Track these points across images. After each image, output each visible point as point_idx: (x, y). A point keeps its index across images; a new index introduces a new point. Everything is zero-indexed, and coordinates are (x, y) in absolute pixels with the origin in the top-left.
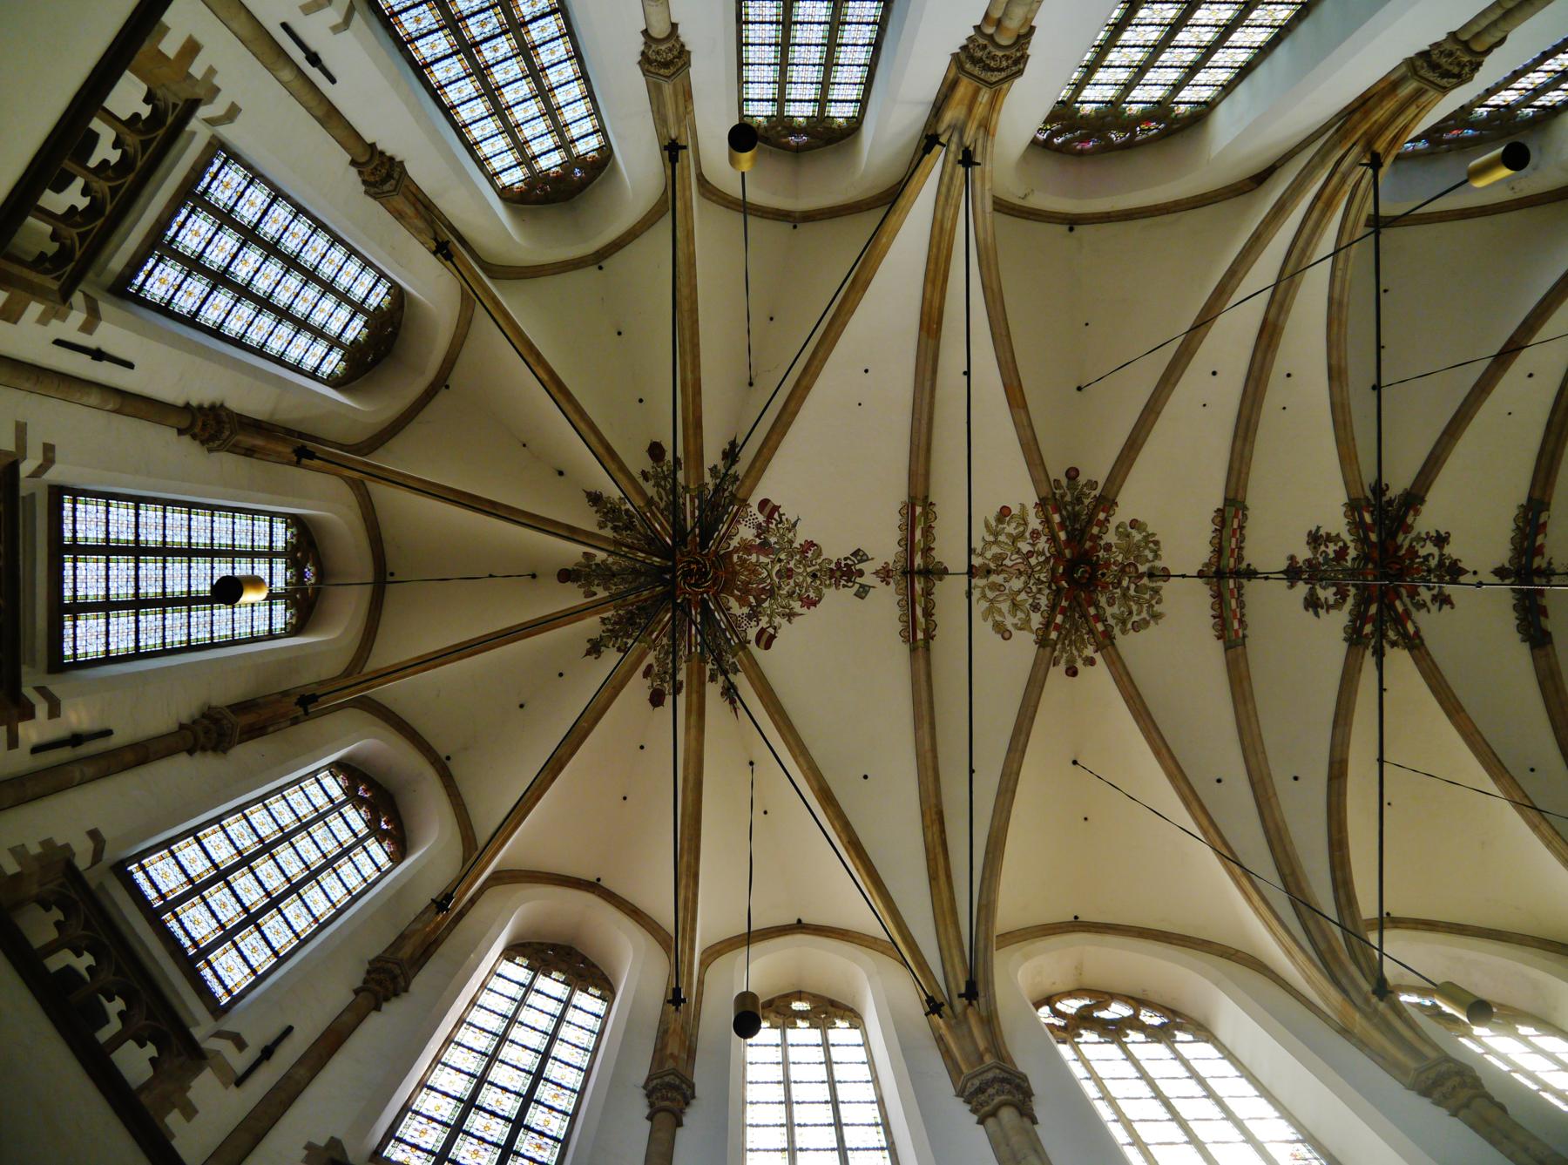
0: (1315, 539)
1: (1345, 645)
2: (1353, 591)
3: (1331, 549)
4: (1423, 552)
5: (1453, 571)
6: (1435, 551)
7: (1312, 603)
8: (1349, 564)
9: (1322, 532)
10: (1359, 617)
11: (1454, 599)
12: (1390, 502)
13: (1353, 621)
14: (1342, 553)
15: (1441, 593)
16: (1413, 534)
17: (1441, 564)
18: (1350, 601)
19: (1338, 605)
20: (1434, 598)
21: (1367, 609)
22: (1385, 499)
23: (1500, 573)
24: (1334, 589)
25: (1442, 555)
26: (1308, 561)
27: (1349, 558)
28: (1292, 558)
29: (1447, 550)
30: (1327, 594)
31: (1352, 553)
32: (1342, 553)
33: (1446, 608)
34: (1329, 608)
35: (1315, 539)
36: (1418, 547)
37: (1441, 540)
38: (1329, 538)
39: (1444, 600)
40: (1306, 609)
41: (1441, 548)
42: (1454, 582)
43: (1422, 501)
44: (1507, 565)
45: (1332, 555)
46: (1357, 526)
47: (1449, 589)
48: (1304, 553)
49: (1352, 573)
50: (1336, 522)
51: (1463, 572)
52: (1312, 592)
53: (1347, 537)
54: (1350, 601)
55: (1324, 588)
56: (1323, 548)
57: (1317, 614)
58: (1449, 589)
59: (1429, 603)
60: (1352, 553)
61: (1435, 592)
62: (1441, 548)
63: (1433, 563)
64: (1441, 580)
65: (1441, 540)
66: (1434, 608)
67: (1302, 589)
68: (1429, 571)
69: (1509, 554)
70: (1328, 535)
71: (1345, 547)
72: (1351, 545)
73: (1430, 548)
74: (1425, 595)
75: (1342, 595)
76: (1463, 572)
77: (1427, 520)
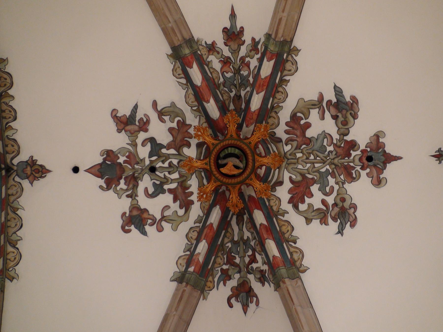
0: (343, 214)
1: (297, 43)
2: (281, 131)
3: (316, 199)
4: (166, 199)
5: (110, 171)
6: (144, 202)
7: (344, 109)
8: (286, 175)
9: (334, 226)
10: (274, 88)
11: (112, 126)
12: (226, 276)
13: (283, 82)
14: (299, 194)
15: (133, 135)
16: (184, 227)
17: (133, 181)
18: (285, 116)
19: (305, 107)
20: (144, 125)
21: (265, 101)
22: (233, 283)
23: (36, 171)
24: (309, 133)
25: (133, 196)
26: (351, 178)
27: (287, 185)
28: (378, 182)
29: (124, 205)
30: (321, 125)
31: (283, 193)
32: (299, 194)
33: (125, 111)
34: (318, 104)
35: (343, 214)
36: (175, 206)
37: (136, 220)
38: (323, 216)
39: (128, 123)
40: (355, 100)
41: (135, 207)
42: (109, 154)
43: (180, 278)
44: (25, 183)
45: (315, 189)
46: (283, 239)
47: (118, 141)
48: (360, 190)
49: (282, 160)
50: (313, 239)
51: (99, 171)
52: (344, 127)
53: (294, 218)
54: (285, 116)
55: (325, 135)
56: (330, 200)
57: (338, 91)
58: (118, 141)
59: (154, 116)
60: (283, 193)
61: (142, 136)
62: (135, 207)
63: (146, 183)
64: (132, 158)
65: (136, 220)
66: (145, 110)
67: (361, 133)
68: (153, 169)
69: (22, 201)
70: (324, 221)
71: (296, 200)
72: (286, 206)
73: (154, 206)
74: (160, 131)
75: (297, 123)
76: (99, 171)
77: (164, 250)
